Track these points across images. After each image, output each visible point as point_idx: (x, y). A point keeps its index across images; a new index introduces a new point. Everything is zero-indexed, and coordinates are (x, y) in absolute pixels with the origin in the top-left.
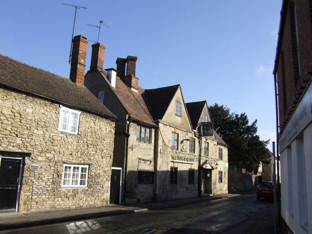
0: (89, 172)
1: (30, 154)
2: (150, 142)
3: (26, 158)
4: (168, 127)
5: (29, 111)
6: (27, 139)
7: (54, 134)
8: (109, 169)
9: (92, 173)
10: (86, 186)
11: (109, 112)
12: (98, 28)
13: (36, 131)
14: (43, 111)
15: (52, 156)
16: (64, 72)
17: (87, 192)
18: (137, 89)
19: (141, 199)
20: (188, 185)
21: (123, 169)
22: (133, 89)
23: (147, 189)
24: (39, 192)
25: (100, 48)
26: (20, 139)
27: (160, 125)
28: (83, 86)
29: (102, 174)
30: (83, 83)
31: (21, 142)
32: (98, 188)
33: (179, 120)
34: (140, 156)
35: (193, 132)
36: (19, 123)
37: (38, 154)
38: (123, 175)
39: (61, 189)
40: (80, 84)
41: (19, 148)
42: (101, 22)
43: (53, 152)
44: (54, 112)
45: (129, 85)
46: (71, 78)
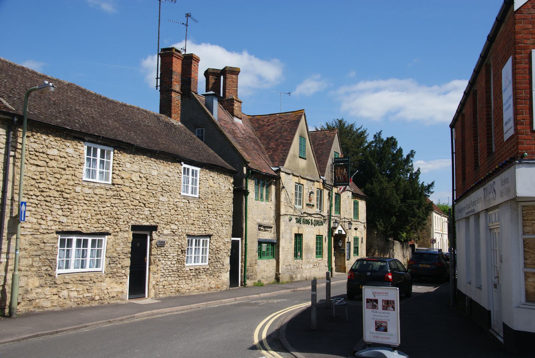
0: (210, 246)
1: (157, 226)
2: (301, 205)
3: (154, 232)
4: (291, 176)
5: (155, 173)
6: (154, 209)
7: (178, 200)
8: (229, 240)
9: (214, 247)
10: (207, 263)
11: (220, 161)
12: (184, 27)
13: (161, 198)
14: (166, 172)
15: (176, 227)
16: (154, 108)
17: (209, 272)
18: (241, 119)
19: (261, 280)
20: (316, 260)
21: (242, 240)
22: (236, 120)
23: (268, 266)
24: (166, 274)
25: (193, 61)
26: (148, 209)
27: (282, 175)
28: (180, 123)
29: (223, 247)
30: (179, 119)
31: (149, 212)
32: (218, 265)
33: (303, 163)
34: (259, 221)
35: (322, 181)
36: (147, 190)
37: (164, 226)
38: (242, 247)
39: (184, 269)
40: (176, 121)
41: (147, 221)
42: (188, 15)
43: (177, 223)
44: (176, 171)
45: (232, 113)
46: (161, 112)
